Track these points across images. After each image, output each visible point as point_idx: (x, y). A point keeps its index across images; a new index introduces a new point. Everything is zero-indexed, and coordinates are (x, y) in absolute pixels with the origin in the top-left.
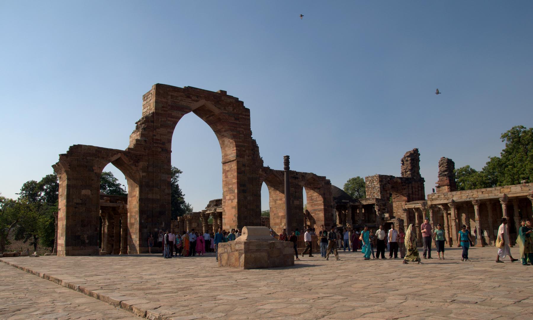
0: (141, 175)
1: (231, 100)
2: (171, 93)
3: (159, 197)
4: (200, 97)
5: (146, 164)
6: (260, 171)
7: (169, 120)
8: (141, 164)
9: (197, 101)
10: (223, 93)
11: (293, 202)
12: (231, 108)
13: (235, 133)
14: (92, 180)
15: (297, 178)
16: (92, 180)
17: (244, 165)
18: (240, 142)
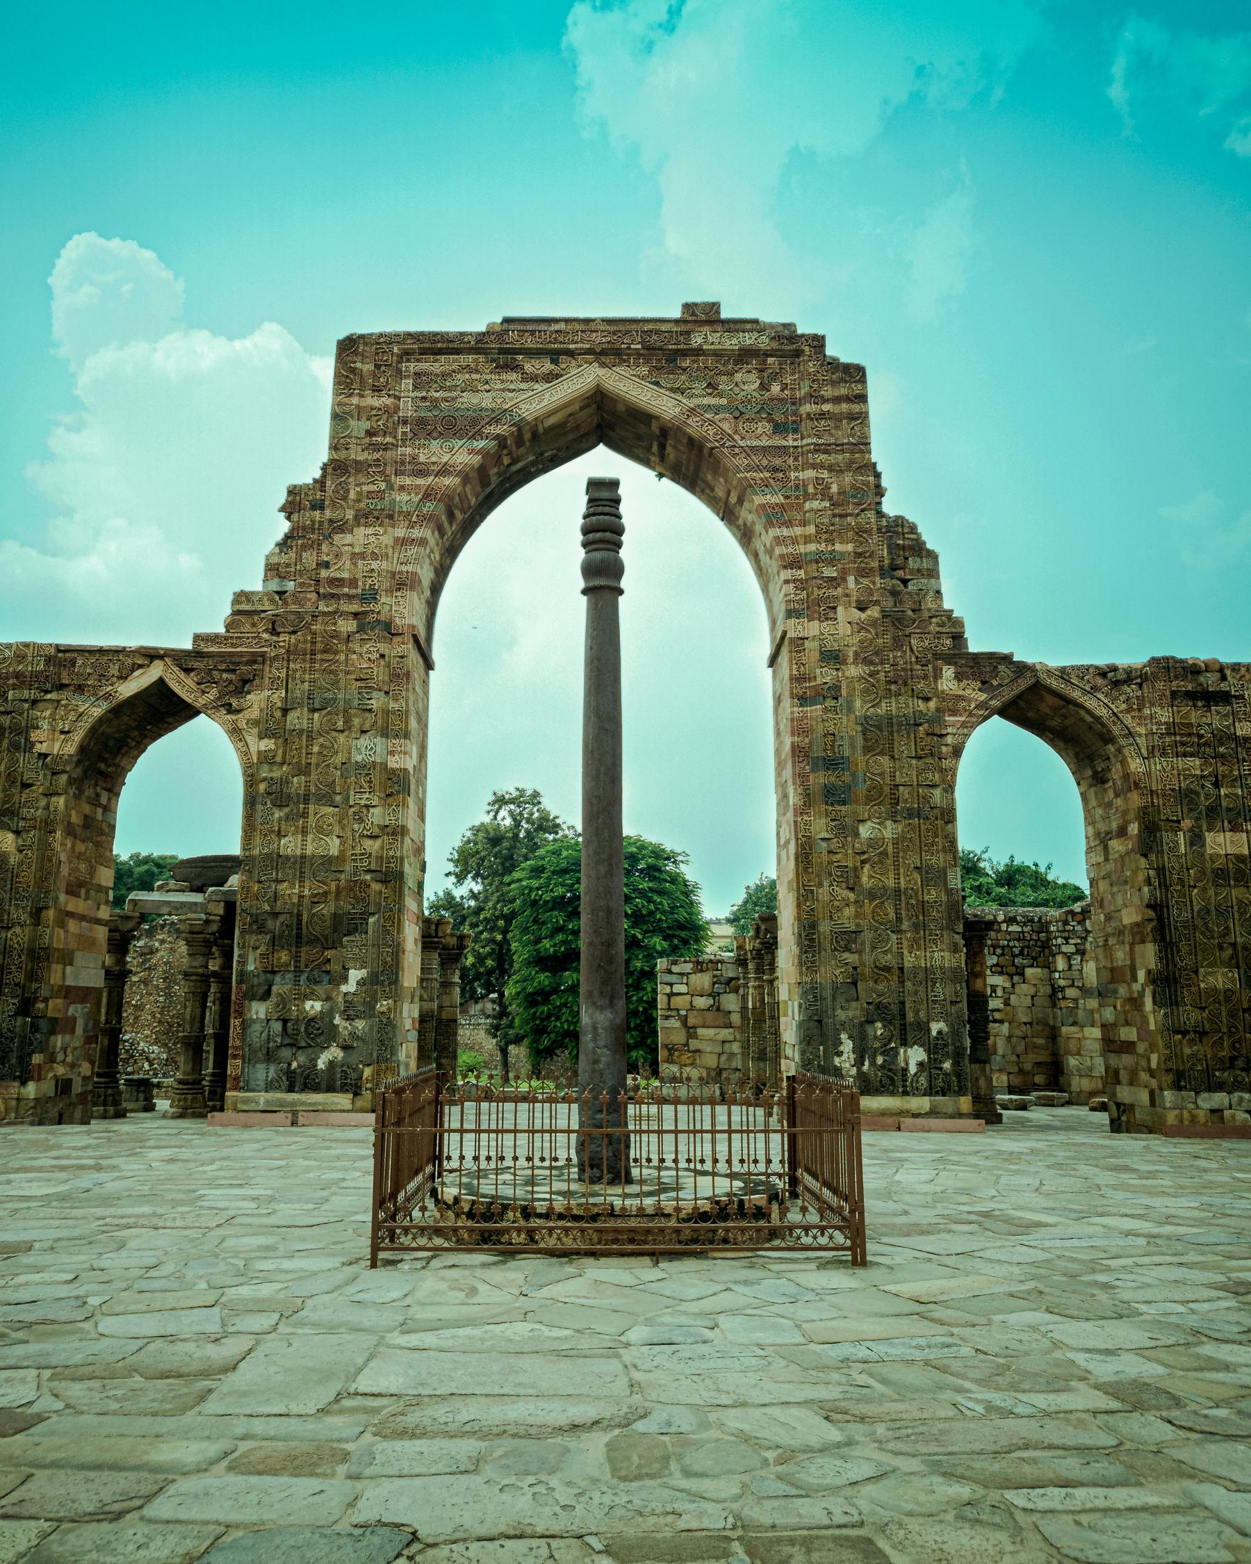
0: (253, 749)
1: (748, 339)
2: (413, 367)
3: (334, 846)
4: (571, 354)
5: (278, 696)
6: (948, 680)
7: (402, 488)
8: (257, 701)
9: (550, 377)
10: (704, 315)
11: (1196, 839)
12: (753, 377)
13: (779, 499)
14: (26, 786)
15: (1225, 698)
16: (26, 786)
17: (832, 657)
18: (807, 539)
